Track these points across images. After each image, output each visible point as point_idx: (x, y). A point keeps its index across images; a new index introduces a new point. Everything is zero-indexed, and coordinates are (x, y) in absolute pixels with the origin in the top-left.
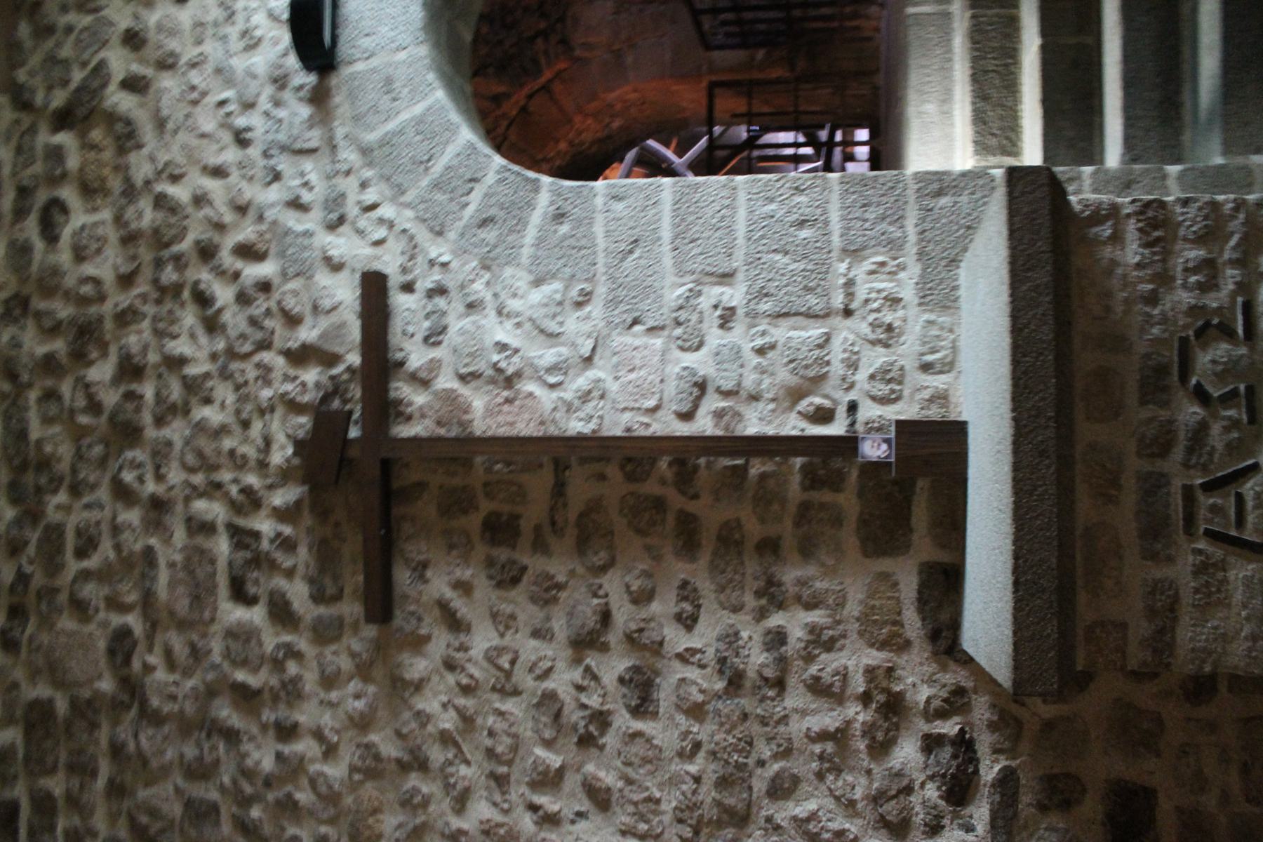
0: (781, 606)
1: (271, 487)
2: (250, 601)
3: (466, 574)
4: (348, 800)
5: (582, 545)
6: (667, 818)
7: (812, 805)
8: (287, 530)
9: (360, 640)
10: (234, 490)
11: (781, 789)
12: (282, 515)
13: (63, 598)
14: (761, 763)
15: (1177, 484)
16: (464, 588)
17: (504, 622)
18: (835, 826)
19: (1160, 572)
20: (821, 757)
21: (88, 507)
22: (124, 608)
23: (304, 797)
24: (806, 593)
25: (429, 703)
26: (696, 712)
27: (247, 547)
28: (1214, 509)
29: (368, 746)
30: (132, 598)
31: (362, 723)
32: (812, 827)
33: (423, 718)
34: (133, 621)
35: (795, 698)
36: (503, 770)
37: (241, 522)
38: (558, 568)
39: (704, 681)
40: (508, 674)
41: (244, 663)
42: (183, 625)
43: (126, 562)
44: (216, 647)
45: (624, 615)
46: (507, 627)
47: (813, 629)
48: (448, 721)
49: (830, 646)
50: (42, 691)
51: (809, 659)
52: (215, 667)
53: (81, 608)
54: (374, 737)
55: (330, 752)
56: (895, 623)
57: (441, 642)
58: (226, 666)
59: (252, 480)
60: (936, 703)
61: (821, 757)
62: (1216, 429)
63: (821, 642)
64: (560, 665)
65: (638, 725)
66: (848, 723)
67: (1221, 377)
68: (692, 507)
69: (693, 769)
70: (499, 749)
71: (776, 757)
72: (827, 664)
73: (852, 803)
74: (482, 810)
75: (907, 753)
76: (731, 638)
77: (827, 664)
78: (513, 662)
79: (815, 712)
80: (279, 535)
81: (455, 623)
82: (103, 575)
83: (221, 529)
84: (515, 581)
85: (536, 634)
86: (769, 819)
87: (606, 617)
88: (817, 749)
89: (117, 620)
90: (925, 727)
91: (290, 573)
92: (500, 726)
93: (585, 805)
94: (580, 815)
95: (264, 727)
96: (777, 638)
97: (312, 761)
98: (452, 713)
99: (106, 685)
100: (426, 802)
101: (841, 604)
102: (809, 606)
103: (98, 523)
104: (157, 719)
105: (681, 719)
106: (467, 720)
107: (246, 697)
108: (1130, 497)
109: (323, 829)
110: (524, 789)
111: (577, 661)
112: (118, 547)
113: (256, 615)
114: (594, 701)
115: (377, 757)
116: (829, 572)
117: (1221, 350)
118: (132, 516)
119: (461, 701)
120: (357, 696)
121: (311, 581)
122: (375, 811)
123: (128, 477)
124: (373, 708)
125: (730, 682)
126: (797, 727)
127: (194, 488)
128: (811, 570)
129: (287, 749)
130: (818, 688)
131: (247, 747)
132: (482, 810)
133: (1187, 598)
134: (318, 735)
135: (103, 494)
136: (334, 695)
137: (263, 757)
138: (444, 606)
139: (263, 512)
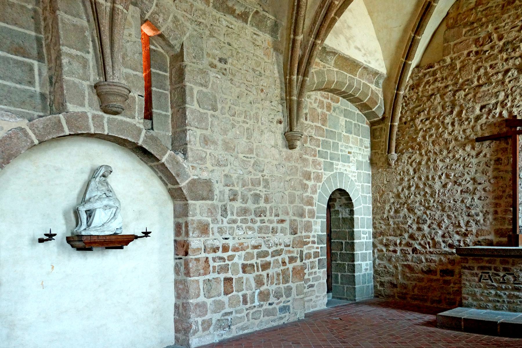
0: (484, 215)
1: (507, 109)
2: (481, 110)
3: (488, 156)
4: (441, 139)
5: (495, 178)
6: (442, 198)
7: (446, 222)
8: (497, 115)
9: (473, 137)
10: (506, 101)
11: (449, 217)
12: (501, 113)
13: (480, 64)
14: (453, 213)
15: (490, 271)
16: (485, 156)
17: (478, 164)
18: (443, 226)
19: (476, 268)
20: (455, 223)
21: (503, 64)
22: (478, 80)
23: (440, 130)
24: (486, 219)
25: (461, 152)
26: (462, 201)
27: (493, 107)
28: (486, 276)
29: (452, 141)
30: (481, 82)
31: (456, 139)
32: (443, 222)
33: (457, 152)
34: (476, 83)
35: (466, 218)
36: (449, 168)
37: (499, 104)
38: (490, 174)
39: (468, 202)
40: (467, 167)
41: (467, 112)
42: (475, 96)
43: (489, 79)
44: (471, 104)
45: (479, 187)
46: (477, 165)
47: (479, 221)
48: (457, 156)
49: (476, 224)
50: (458, 67)
51: (474, 220)
52: (466, 105)
53: (478, 69)
54: (453, 142)
55: (450, 134)
56: (481, 235)
57: (474, 153)
58: (466, 108)
59: (509, 104)
60: (466, 242)
61: (455, 223)
62: (499, 277)
63: (477, 222)
64: (470, 176)
65: (459, 191)
66: (462, 227)
67: (508, 279)
68: (504, 198)
69: (452, 201)
70: (453, 167)
71: (455, 216)
72: (472, 223)
73: (447, 228)
74: (440, 164)
75: (457, 237)
76: (477, 206)
77: (472, 223)
78: (470, 167)
79: (464, 222)
80: (496, 114)
81: (478, 155)
82: (486, 73)
83: (497, 100)
84: (487, 166)
85: (476, 170)
86: (443, 215)
87: (480, 184)
88: (457, 222)
89: (475, 80)
90: (462, 240)
91: (487, 118)
92: (457, 166)
93: (443, 183)
94: (442, 182)
95: (454, 119)
96: (477, 215)
97: (448, 131)
98: (459, 157)
99: (461, 81)
100: (441, 154)
101: (484, 225)
102: (484, 220)
103: (498, 68)
104: (454, 95)
105: (461, 199)
106: (458, 160)
107: (460, 113)
108: (487, 265)
109: (435, 135)
110: (446, 172)
111: (471, 179)
112: (492, 75)
113: (477, 112)
114: (463, 183)
115: (450, 143)
116: (491, 223)
117: (512, 279)
118: (500, 76)
119: (462, 158)
120: (461, 137)
121: (485, 123)
122: (439, 145)
123: (510, 74)
124: (459, 141)
125: (469, 207)
126: (460, 218)
127: (507, 91)
128: (491, 220)
129: (450, 125)
130: (468, 222)
131: (449, 116)
132: (440, 164)
133: (472, 271)
134: (453, 131)
135: (506, 67)
136: (461, 133)
137: (448, 120)
138: (481, 152)
139: (501, 109)
